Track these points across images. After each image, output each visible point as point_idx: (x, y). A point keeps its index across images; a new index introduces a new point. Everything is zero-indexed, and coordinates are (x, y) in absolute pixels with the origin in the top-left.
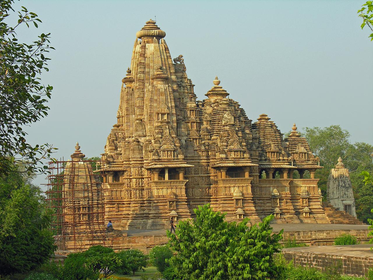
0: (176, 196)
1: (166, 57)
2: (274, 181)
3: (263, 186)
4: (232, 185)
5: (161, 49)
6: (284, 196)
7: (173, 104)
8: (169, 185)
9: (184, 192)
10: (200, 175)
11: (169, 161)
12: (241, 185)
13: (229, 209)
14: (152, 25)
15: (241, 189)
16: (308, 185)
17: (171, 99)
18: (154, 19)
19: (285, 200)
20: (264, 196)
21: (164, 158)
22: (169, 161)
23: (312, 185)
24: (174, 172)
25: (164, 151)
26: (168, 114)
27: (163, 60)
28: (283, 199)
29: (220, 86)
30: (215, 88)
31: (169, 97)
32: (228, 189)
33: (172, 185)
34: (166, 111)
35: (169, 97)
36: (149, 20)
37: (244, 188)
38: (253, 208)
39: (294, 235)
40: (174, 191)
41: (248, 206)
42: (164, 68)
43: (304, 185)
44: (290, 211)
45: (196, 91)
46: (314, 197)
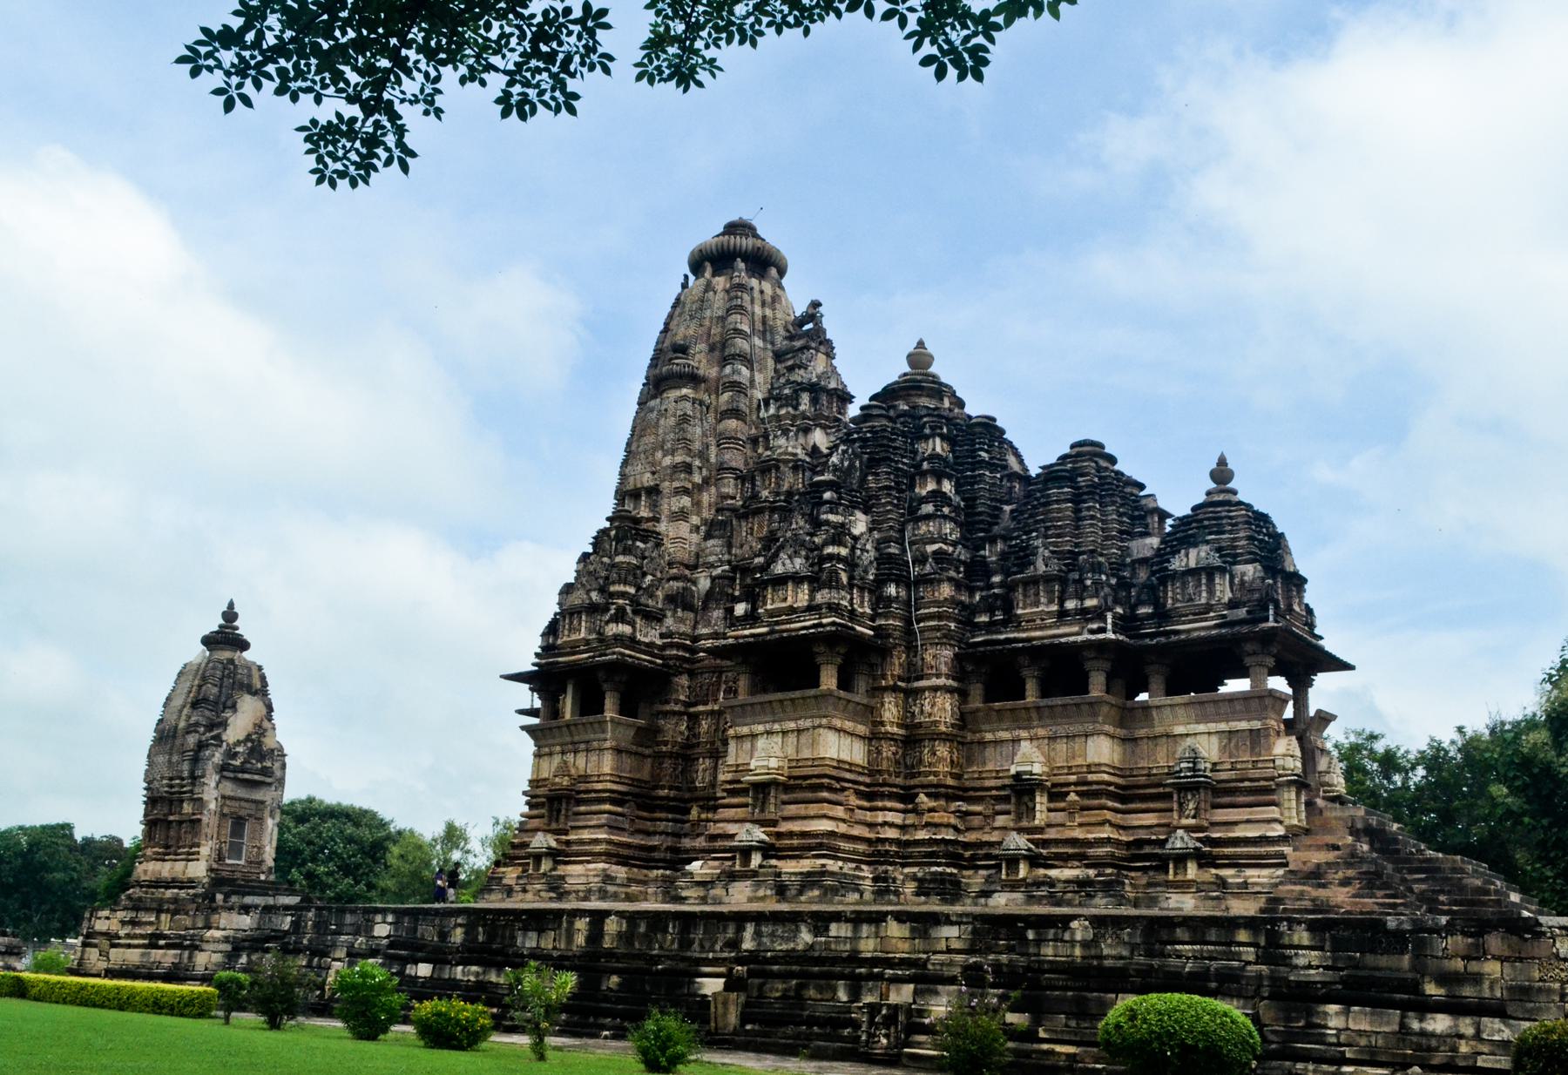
2: (1034, 715)
3: (989, 736)
4: (761, 728)
6: (1073, 778)
8: (568, 739)
12: (792, 725)
15: (792, 738)
16: (1223, 726)
19: (1073, 797)
20: (988, 783)
23: (1243, 725)
28: (1068, 793)
33: (576, 738)
37: (804, 738)
39: (665, 931)
41: (803, 813)
43: (1202, 728)
44: (1091, 851)
46: (1247, 784)
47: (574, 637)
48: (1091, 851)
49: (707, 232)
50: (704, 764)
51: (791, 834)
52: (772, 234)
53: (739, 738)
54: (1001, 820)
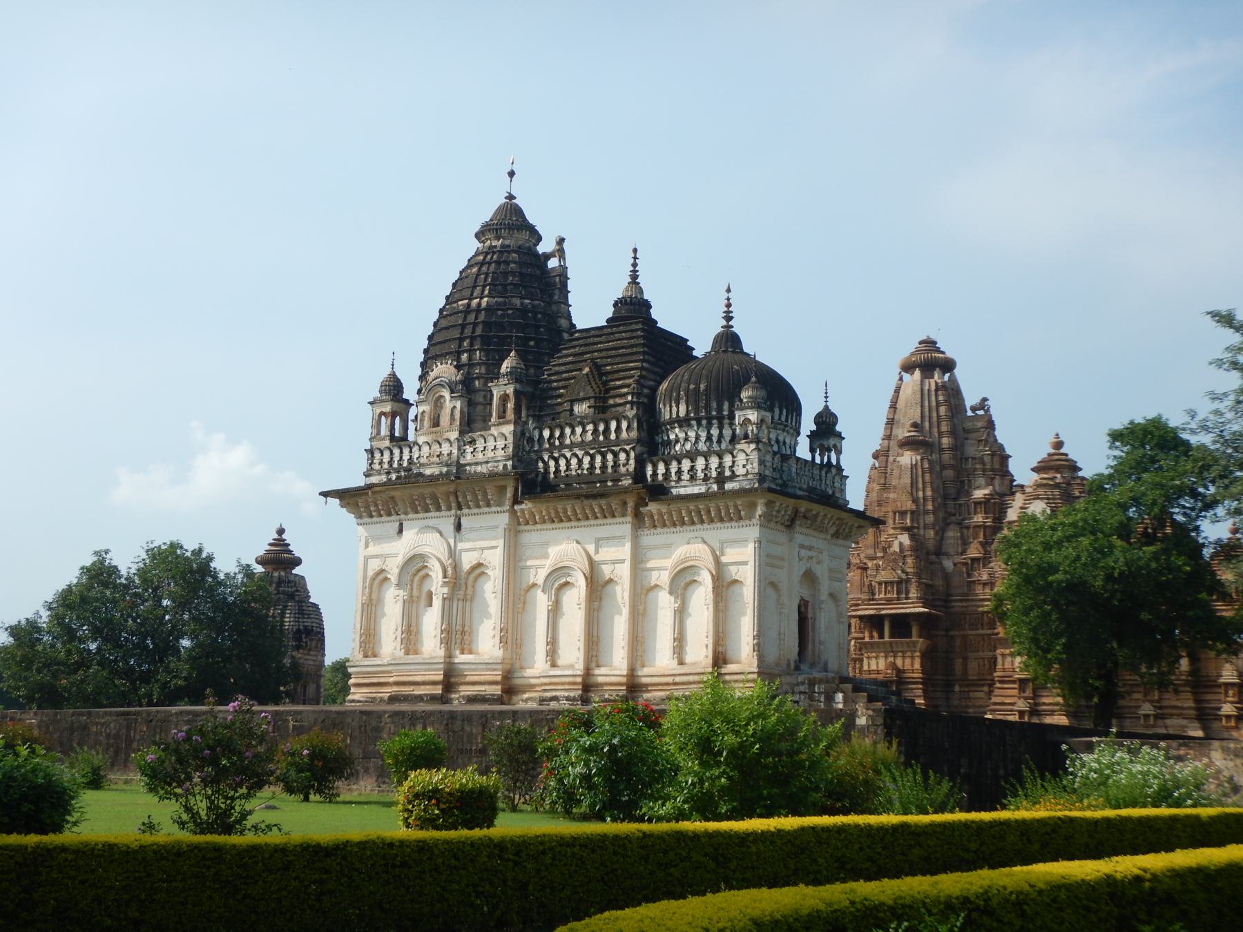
0: (899, 672)
1: (934, 404)
5: (926, 388)
7: (929, 493)
9: (917, 665)
10: (981, 632)
11: (889, 601)
13: (1008, 701)
14: (930, 344)
17: (924, 482)
18: (933, 337)
21: (882, 596)
22: (889, 601)
24: (901, 625)
25: (880, 583)
26: (912, 512)
27: (927, 409)
29: (1062, 451)
30: (1049, 455)
31: (920, 480)
32: (1009, 659)
34: (909, 505)
35: (920, 480)
36: (924, 337)
38: (1060, 700)
40: (899, 662)
42: (927, 424)
45: (1013, 466)
47: (889, 596)
48: (1185, 712)
49: (907, 348)
50: (959, 662)
51: (1044, 704)
52: (949, 349)
53: (1003, 655)
54: (1136, 696)
